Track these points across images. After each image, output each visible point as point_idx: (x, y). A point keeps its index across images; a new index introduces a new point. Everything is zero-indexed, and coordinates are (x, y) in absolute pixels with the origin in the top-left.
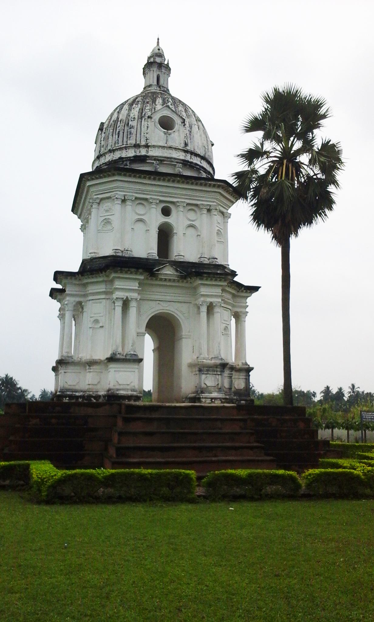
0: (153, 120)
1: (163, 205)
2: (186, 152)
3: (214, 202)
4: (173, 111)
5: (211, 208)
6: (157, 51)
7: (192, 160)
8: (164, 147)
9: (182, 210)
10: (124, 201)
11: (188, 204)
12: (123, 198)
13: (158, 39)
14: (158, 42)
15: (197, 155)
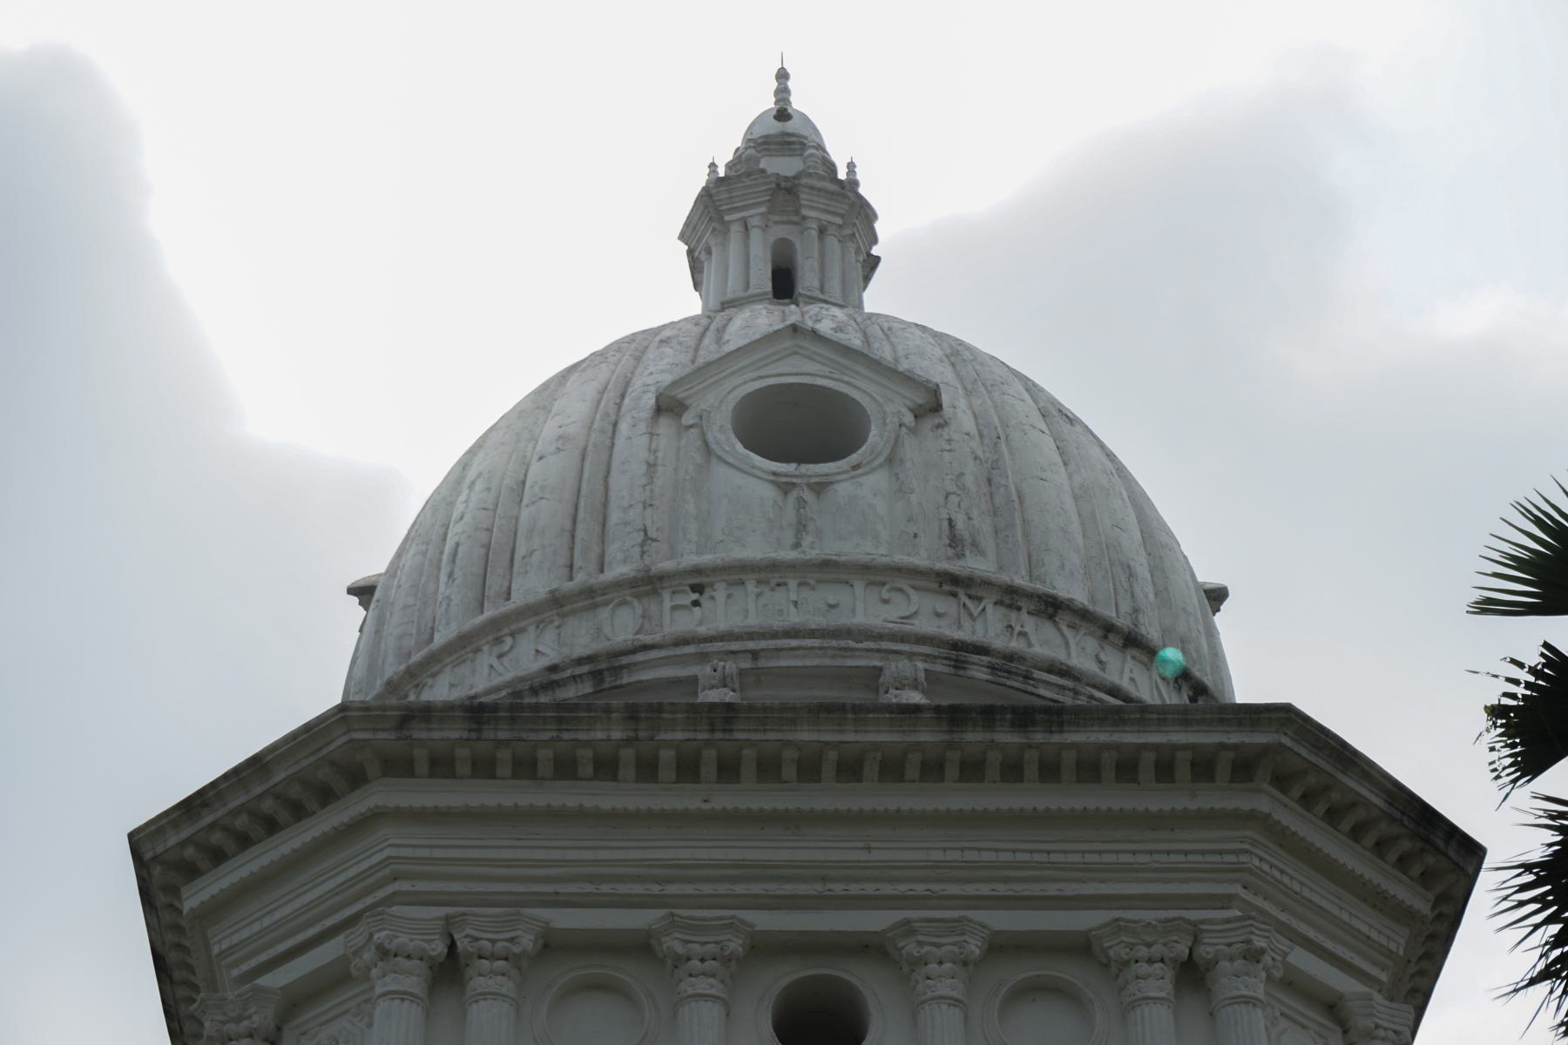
0: (687, 419)
1: (782, 977)
2: (952, 584)
3: (1225, 901)
4: (846, 351)
5: (1205, 951)
6: (776, 127)
7: (1015, 645)
8: (774, 566)
9: (949, 987)
10: (448, 971)
11: (1001, 947)
12: (439, 948)
13: (782, 75)
14: (782, 93)
15: (1051, 607)
